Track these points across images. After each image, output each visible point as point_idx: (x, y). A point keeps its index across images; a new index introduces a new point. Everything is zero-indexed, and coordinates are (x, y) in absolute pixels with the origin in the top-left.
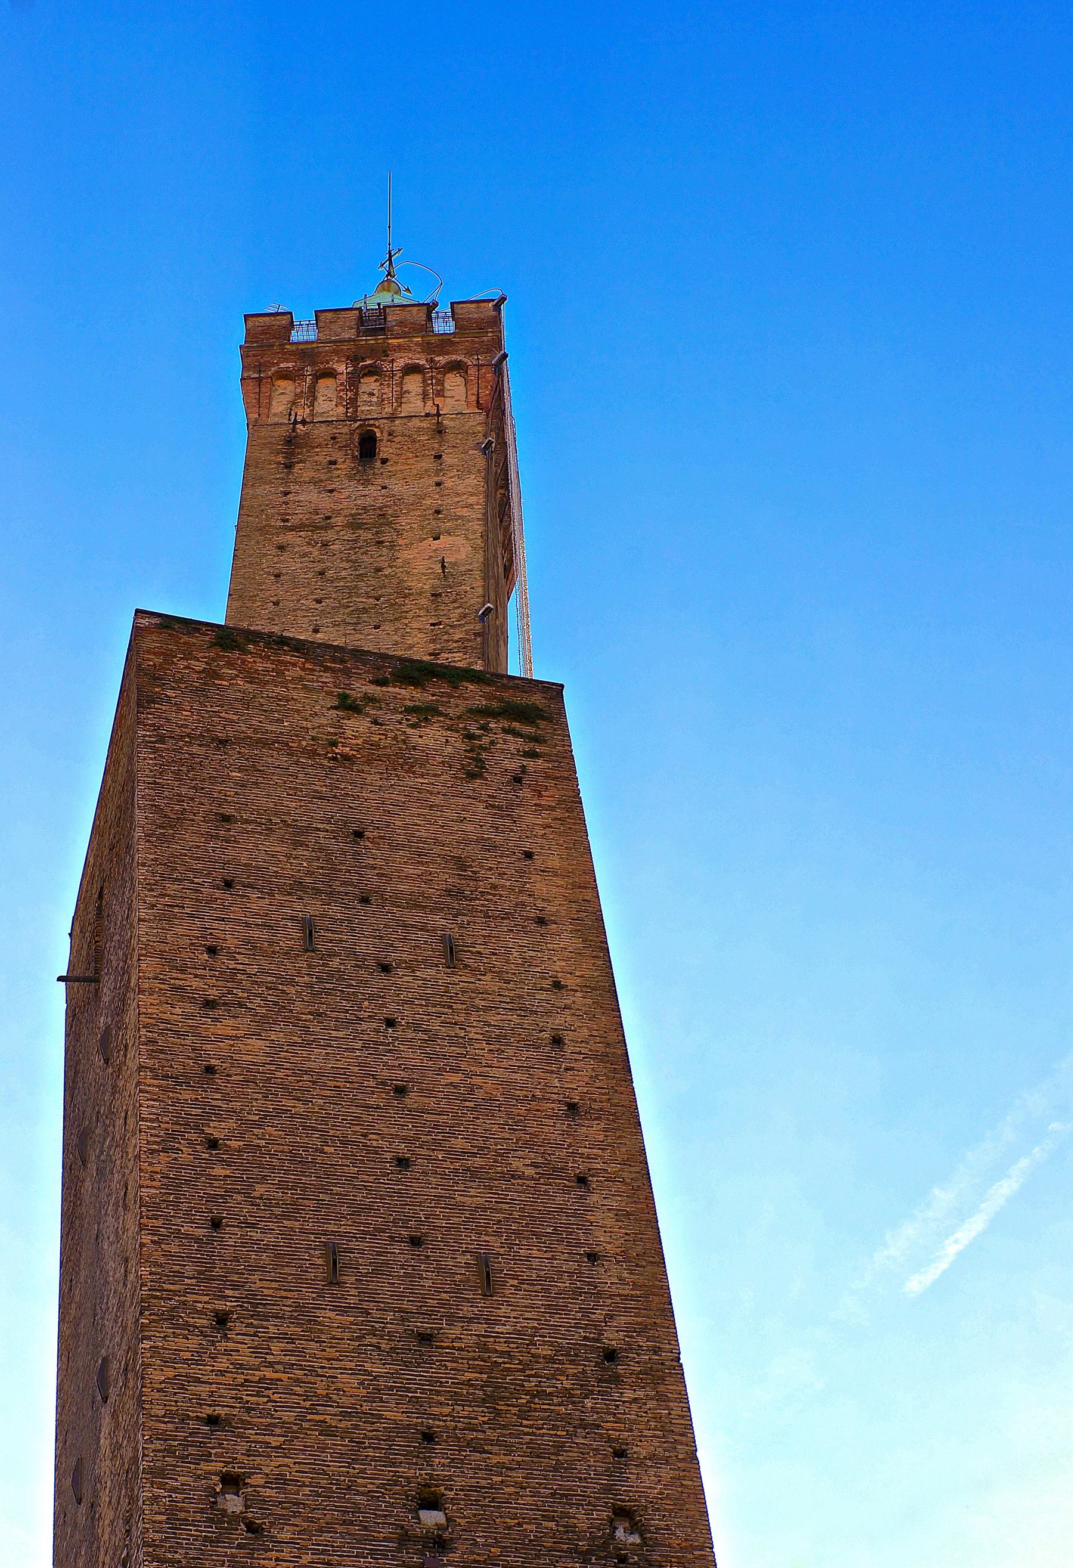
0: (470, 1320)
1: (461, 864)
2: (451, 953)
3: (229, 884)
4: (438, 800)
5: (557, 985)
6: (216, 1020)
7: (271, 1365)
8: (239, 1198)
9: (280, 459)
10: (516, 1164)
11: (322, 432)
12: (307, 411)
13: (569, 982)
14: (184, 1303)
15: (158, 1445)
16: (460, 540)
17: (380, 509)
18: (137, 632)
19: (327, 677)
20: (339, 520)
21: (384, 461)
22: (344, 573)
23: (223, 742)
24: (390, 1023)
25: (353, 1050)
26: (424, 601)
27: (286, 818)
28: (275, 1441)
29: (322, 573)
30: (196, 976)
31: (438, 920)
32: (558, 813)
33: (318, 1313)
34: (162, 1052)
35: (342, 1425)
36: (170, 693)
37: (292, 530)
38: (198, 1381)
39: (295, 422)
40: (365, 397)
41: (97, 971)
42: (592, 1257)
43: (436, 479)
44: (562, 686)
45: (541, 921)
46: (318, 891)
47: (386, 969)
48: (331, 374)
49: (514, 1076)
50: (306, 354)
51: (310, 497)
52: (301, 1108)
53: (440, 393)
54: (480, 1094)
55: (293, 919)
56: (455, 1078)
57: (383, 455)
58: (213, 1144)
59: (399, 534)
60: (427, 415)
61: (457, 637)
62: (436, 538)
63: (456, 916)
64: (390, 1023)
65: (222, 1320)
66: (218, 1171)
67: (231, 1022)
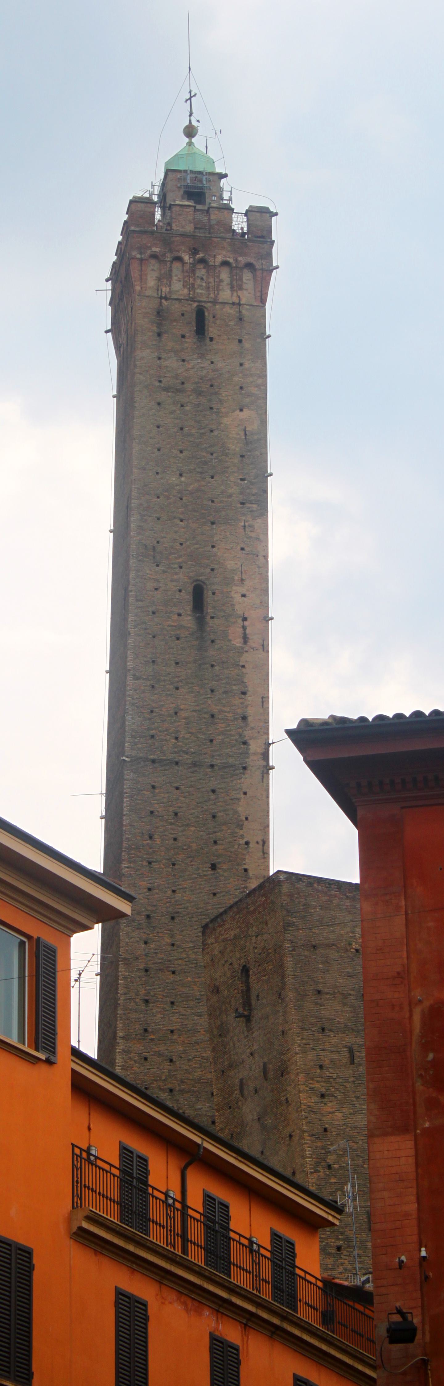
9: (155, 328)
11: (176, 308)
12: (168, 289)
17: (211, 380)
20: (188, 386)
21: (211, 339)
22: (193, 431)
27: (340, 990)
30: (317, 1082)
37: (164, 390)
40: (199, 281)
48: (179, 259)
51: (172, 363)
53: (240, 288)
57: (211, 335)
60: (233, 304)
62: (241, 410)
65: (339, 1248)
66: (333, 1180)
67: (330, 1104)
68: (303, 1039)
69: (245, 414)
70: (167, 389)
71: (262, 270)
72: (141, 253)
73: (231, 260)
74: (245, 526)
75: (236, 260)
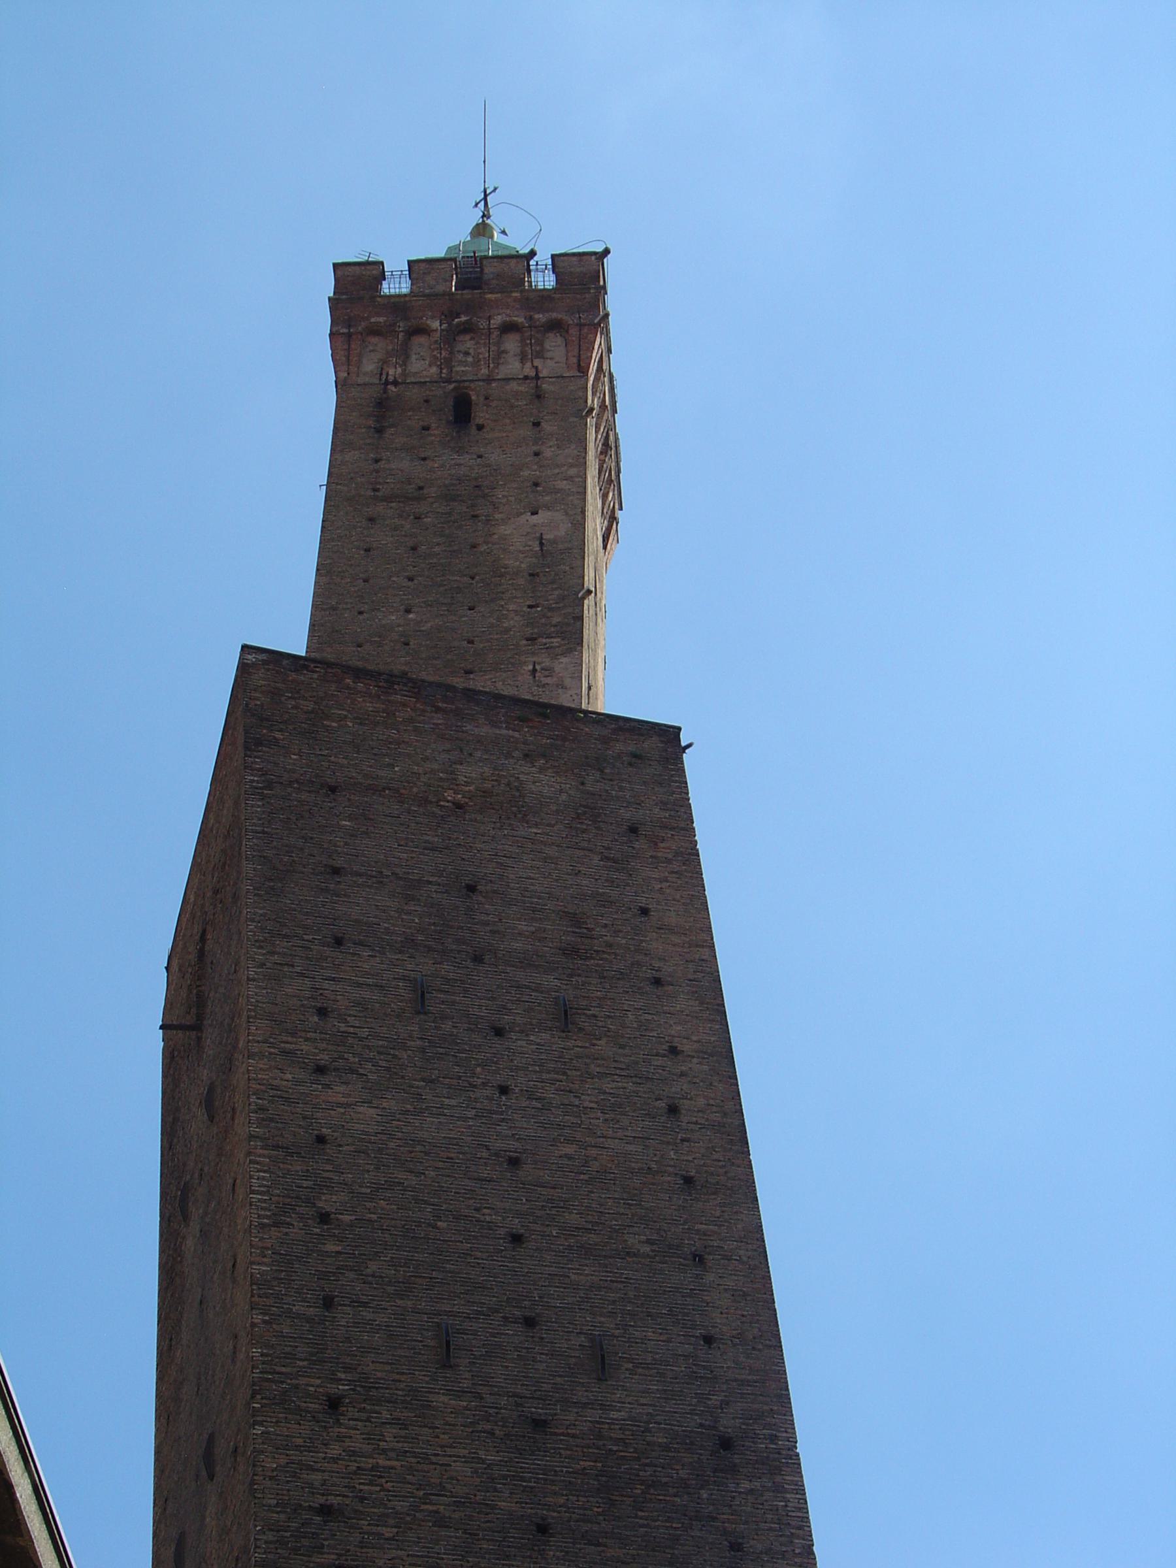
0: (585, 1405)
1: (576, 920)
2: (565, 1017)
3: (339, 942)
4: (551, 851)
5: (674, 1051)
6: (327, 1086)
7: (384, 1451)
8: (352, 1275)
9: (371, 422)
10: (631, 1241)
12: (399, 370)
13: (686, 1047)
14: (296, 1387)
15: (270, 1536)
16: (558, 516)
17: (476, 479)
18: (244, 669)
19: (439, 719)
20: (432, 491)
21: (480, 428)
22: (437, 549)
23: (333, 789)
24: (504, 1090)
25: (466, 1119)
26: (521, 581)
27: (398, 870)
28: (388, 1532)
29: (414, 549)
30: (307, 1039)
31: (550, 981)
32: (675, 866)
33: (431, 1397)
34: (272, 1120)
35: (456, 1516)
36: (278, 735)
37: (382, 501)
38: (312, 1469)
39: (387, 383)
40: (460, 357)
41: (200, 1017)
42: (708, 1340)
43: (535, 448)
44: (679, 729)
45: (657, 982)
46: (430, 949)
47: (499, 1032)
49: (631, 1148)
50: (398, 305)
52: (413, 1180)
53: (540, 355)
54: (595, 1165)
55: (404, 978)
56: (569, 1150)
57: (480, 422)
58: (324, 1218)
59: (495, 506)
60: (526, 378)
61: (555, 620)
62: (534, 513)
63: (571, 975)
64: (504, 1090)
65: (334, 1404)
66: (331, 1247)
67: (342, 1088)
68: (273, 953)
69: (542, 517)
70: (388, 499)
71: (581, 326)
72: (349, 327)
73: (521, 320)
74: (534, 671)
75: (531, 318)
